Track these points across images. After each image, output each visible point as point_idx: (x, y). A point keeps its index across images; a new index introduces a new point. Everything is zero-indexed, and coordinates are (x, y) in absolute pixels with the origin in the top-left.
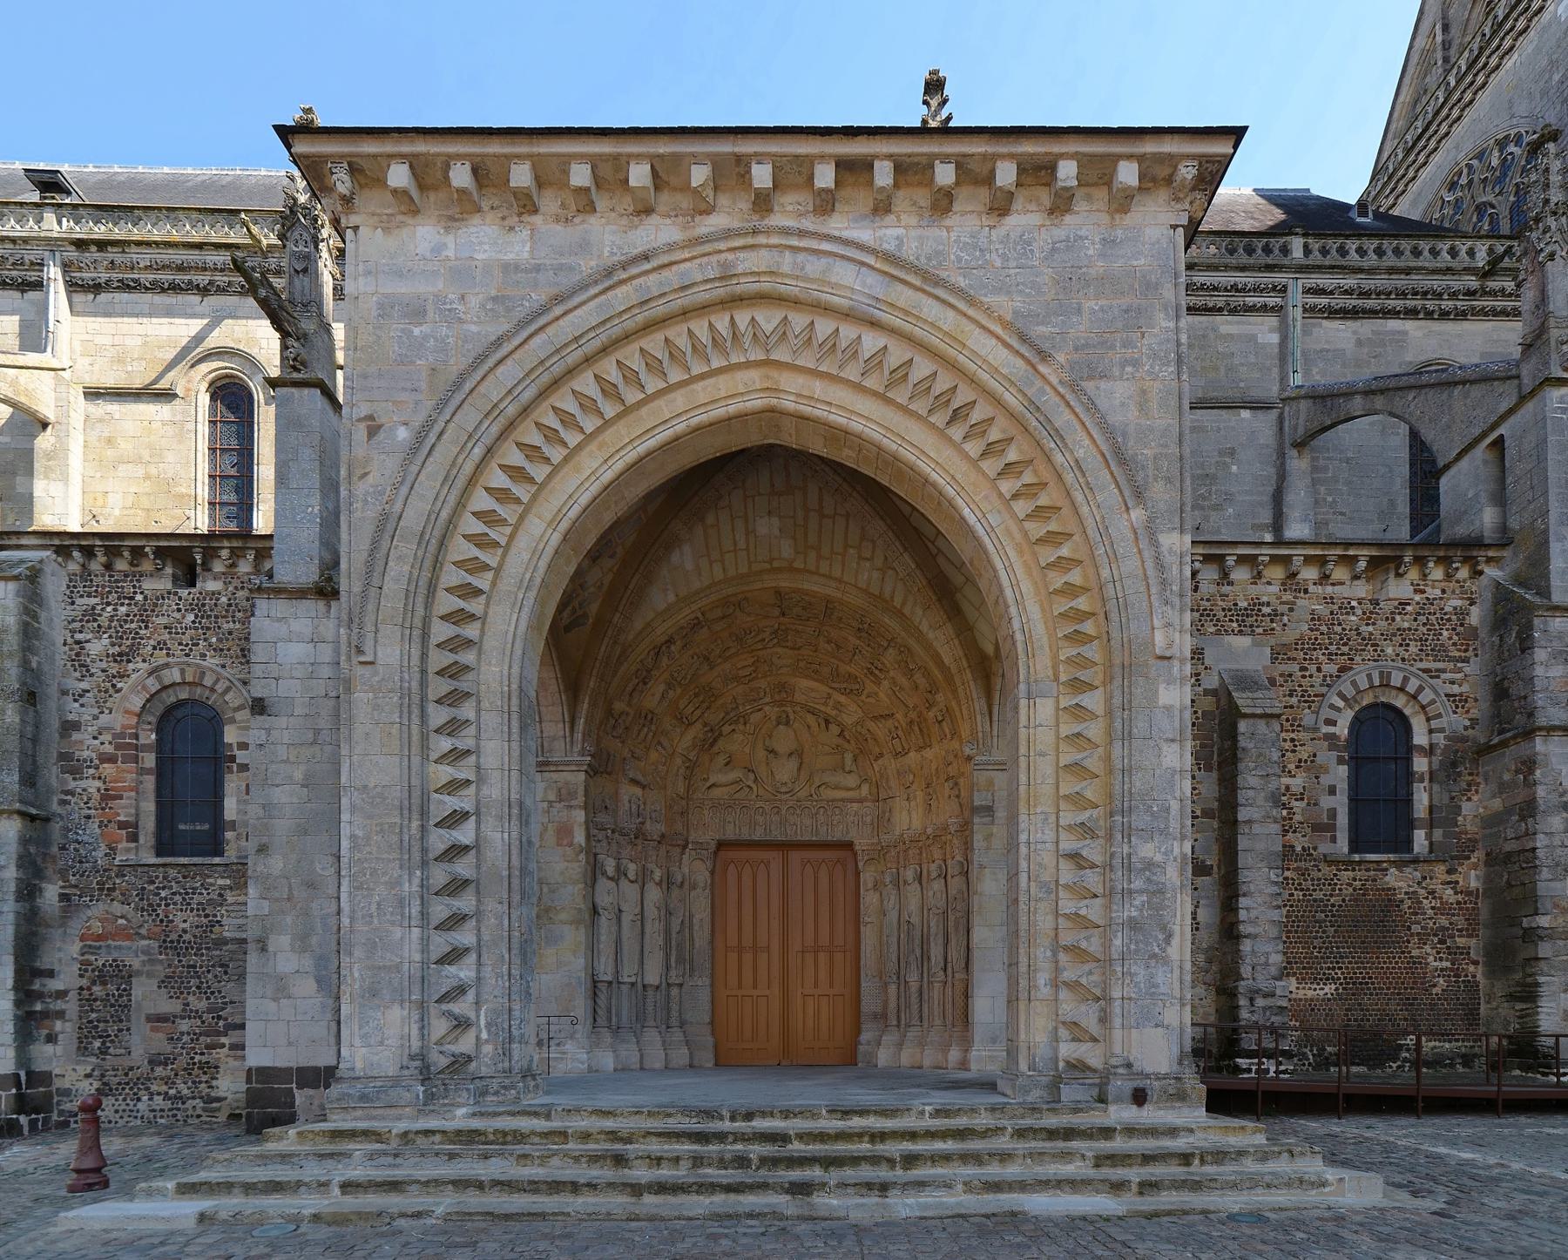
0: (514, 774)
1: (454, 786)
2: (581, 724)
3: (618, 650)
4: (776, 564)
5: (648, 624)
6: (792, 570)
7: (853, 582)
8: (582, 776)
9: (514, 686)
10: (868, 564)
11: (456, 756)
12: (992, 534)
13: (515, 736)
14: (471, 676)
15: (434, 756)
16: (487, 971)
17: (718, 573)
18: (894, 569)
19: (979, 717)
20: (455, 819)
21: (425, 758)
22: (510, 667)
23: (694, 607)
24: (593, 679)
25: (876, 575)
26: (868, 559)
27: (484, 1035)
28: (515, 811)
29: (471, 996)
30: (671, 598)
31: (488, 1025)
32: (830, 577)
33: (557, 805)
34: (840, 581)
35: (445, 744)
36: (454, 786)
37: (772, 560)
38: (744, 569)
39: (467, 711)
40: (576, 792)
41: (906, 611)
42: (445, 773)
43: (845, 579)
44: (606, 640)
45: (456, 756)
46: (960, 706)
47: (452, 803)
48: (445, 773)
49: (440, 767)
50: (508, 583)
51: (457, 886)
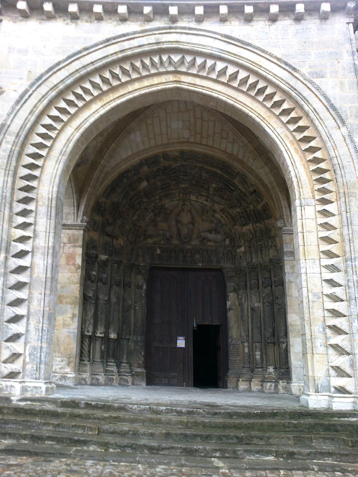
0: (52, 235)
1: (23, 239)
2: (82, 208)
3: (102, 175)
4: (181, 140)
5: (117, 164)
6: (188, 142)
7: (218, 148)
8: (82, 232)
9: (54, 196)
10: (225, 141)
11: (24, 226)
12: (279, 137)
13: (53, 217)
14: (35, 191)
15: (14, 225)
16: (32, 327)
17: (153, 143)
18: (237, 143)
19: (284, 209)
20: (22, 254)
21: (10, 225)
22: (53, 187)
23: (141, 157)
24: (90, 188)
25: (229, 145)
26: (225, 138)
27: (27, 360)
28: (51, 251)
29: (22, 339)
30: (130, 153)
31: (30, 355)
32: (207, 145)
33: (68, 245)
34: (212, 147)
35: (20, 220)
36: (23, 239)
37: (179, 138)
38: (165, 141)
39: (31, 207)
40: (78, 239)
41: (245, 160)
42: (19, 233)
43: (215, 146)
44: (97, 171)
45: (24, 226)
46: (274, 203)
47: (21, 247)
48: (19, 233)
49: (16, 230)
50: (55, 152)
51: (19, 286)
